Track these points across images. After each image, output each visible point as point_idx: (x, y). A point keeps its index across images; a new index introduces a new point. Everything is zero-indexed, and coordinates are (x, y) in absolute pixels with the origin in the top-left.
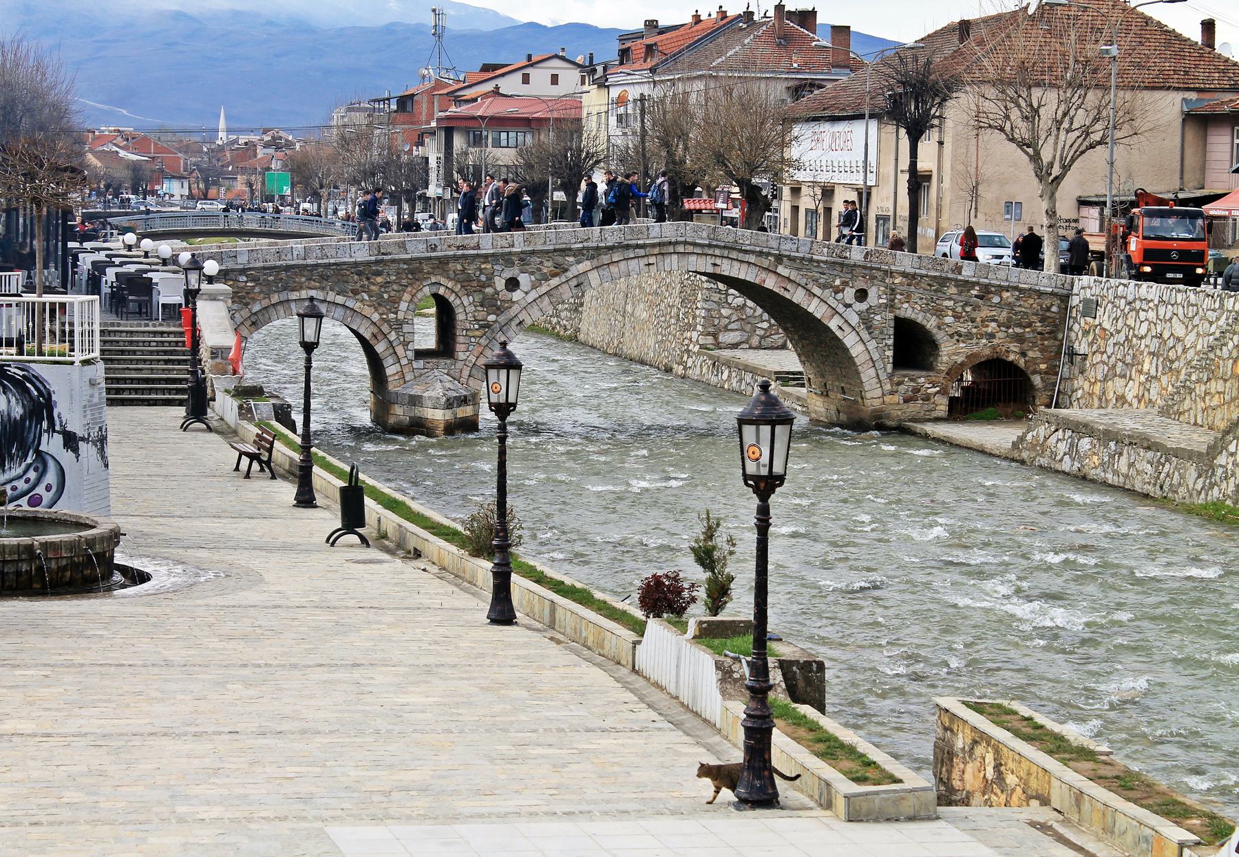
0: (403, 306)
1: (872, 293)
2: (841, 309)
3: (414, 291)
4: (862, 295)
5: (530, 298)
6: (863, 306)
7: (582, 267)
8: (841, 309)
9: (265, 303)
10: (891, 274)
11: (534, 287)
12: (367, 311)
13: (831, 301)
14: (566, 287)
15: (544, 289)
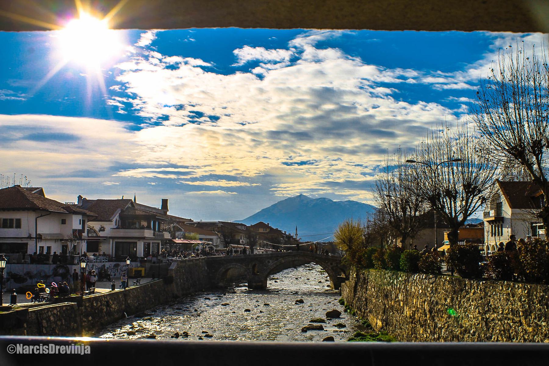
0: (250, 266)
1: (333, 263)
2: (327, 266)
4: (331, 264)
5: (272, 264)
6: (332, 266)
8: (327, 266)
10: (336, 260)
11: (273, 262)
12: (244, 267)
13: (326, 265)
15: (274, 263)
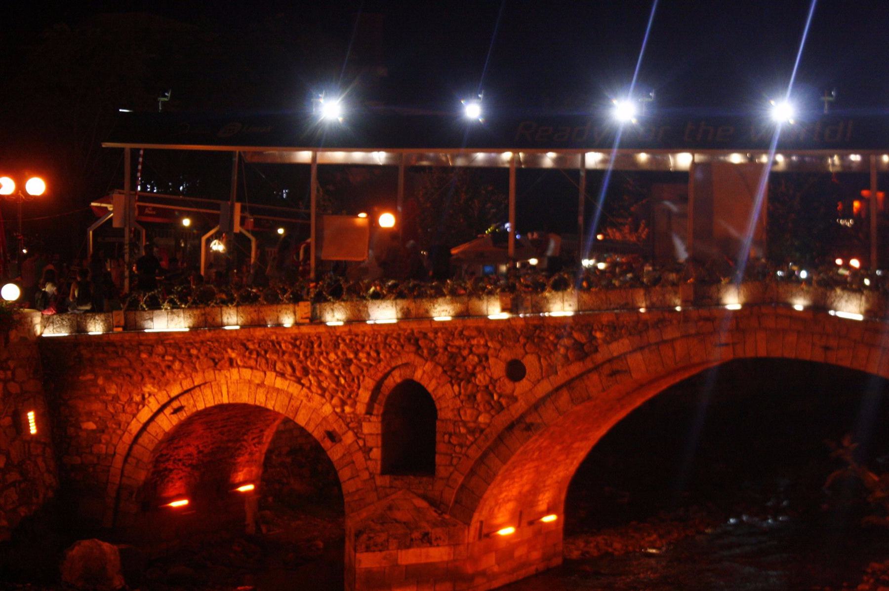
3: (380, 375)
7: (617, 348)
9: (187, 384)
14: (594, 377)
15: (561, 377)
